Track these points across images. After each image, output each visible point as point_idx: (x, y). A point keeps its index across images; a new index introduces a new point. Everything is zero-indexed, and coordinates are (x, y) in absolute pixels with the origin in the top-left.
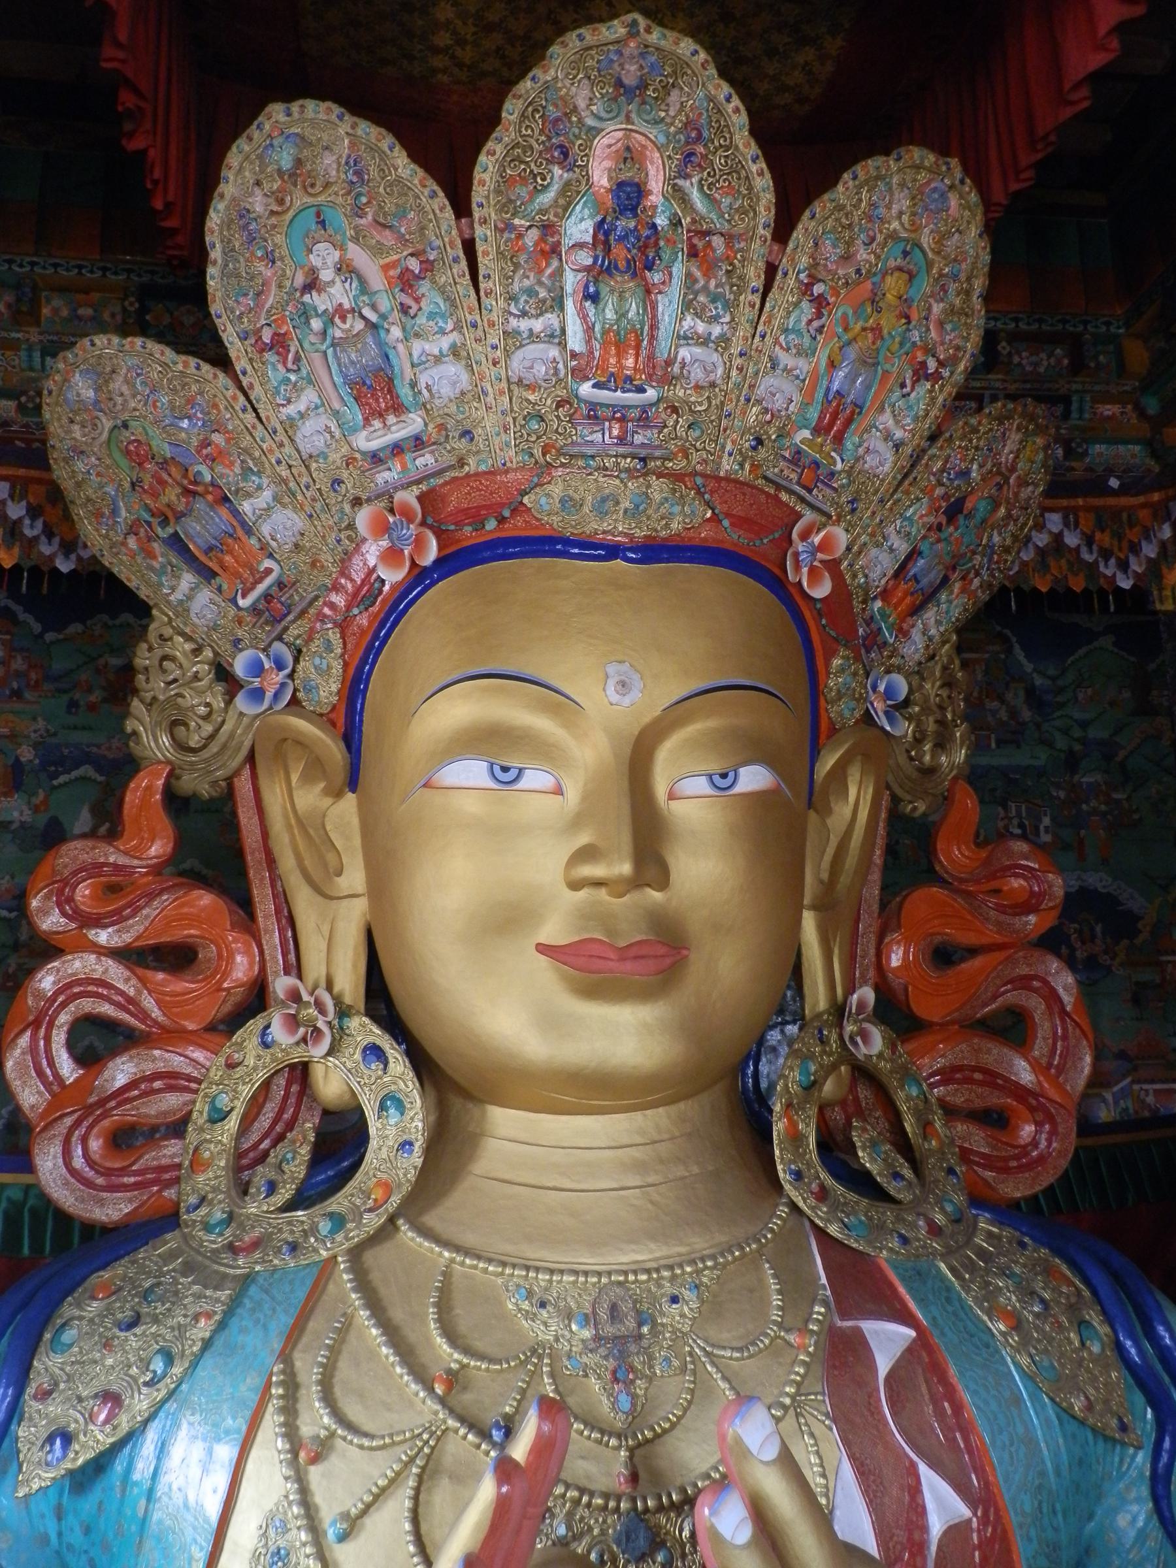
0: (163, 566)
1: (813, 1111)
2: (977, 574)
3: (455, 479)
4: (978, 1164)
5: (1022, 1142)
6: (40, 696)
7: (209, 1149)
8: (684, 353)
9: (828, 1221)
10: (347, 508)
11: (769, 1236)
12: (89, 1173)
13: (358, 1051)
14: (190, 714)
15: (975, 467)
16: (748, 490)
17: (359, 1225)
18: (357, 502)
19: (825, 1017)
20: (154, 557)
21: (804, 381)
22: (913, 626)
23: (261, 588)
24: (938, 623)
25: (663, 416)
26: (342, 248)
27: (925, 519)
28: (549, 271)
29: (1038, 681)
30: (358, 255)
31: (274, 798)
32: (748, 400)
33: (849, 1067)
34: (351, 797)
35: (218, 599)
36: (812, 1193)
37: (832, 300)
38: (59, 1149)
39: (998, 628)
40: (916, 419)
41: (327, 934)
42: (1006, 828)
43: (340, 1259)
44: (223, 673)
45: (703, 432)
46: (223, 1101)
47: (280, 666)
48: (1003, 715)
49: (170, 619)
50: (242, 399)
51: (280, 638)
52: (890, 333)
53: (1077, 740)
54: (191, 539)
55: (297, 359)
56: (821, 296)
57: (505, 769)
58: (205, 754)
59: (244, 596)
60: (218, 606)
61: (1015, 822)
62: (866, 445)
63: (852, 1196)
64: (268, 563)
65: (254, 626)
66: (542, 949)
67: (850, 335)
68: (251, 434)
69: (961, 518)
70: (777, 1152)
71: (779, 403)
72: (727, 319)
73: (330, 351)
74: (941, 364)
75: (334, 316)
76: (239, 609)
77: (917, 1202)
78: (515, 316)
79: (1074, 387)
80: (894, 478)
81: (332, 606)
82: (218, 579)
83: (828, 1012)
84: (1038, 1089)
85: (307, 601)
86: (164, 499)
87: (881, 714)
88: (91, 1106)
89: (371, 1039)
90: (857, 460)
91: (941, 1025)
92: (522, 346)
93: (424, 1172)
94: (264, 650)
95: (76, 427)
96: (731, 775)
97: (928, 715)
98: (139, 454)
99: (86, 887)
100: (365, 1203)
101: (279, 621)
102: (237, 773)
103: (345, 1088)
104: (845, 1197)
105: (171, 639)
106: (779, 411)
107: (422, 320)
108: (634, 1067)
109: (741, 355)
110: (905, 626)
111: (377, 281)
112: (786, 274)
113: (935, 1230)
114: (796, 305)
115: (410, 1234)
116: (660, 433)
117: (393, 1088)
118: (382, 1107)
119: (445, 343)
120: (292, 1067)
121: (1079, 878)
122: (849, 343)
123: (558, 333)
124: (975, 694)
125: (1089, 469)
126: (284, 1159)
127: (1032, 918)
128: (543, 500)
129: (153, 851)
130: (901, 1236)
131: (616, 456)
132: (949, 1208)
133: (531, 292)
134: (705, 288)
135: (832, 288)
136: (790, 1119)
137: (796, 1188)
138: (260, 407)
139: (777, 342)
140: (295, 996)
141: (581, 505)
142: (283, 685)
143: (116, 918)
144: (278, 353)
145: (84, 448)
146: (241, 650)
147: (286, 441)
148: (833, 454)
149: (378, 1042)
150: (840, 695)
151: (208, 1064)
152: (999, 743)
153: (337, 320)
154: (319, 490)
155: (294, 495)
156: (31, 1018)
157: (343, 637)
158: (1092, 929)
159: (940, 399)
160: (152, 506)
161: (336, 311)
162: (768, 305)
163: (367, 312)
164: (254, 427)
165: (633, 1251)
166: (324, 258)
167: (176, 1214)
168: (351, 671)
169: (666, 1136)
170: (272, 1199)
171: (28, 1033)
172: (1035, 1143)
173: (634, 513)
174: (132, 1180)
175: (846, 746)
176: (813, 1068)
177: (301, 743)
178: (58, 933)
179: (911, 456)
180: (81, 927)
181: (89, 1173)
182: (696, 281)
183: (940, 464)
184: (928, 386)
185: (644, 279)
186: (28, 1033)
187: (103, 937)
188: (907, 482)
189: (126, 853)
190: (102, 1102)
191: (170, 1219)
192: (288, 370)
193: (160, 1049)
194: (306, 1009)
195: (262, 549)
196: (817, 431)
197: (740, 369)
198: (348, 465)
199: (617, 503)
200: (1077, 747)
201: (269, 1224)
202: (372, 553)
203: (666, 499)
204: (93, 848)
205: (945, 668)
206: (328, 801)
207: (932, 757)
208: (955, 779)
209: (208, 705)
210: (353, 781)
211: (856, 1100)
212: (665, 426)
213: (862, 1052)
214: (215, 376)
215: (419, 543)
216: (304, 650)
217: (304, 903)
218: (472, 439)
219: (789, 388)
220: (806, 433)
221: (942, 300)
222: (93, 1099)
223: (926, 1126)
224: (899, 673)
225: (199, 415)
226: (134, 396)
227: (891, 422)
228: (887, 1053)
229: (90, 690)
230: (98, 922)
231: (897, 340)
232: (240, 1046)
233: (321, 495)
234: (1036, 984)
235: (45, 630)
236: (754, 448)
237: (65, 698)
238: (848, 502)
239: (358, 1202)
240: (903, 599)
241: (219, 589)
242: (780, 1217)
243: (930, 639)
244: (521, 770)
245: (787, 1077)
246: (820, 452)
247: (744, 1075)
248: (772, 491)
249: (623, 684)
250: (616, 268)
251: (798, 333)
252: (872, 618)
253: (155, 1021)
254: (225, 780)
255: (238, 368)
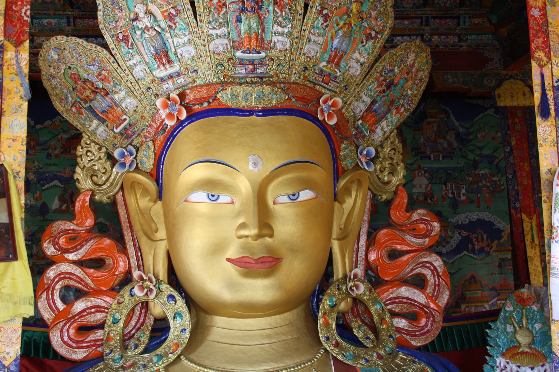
0: (86, 118)
1: (335, 315)
2: (402, 106)
3: (193, 87)
4: (404, 334)
5: (421, 325)
6: (35, 152)
7: (113, 333)
8: (275, 39)
9: (338, 354)
10: (153, 98)
11: (315, 360)
12: (70, 343)
13: (166, 297)
14: (98, 172)
15: (396, 68)
16: (301, 87)
17: (168, 359)
18: (157, 95)
19: (341, 280)
20: (83, 115)
21: (322, 45)
22: (376, 128)
23: (122, 126)
24: (388, 126)
25: (268, 62)
26: (147, 5)
27: (377, 89)
28: (222, 13)
29: (461, 130)
30: (153, 8)
31: (131, 201)
32: (300, 54)
33: (351, 299)
34: (160, 202)
35: (107, 130)
36: (333, 345)
37: (331, 15)
38: (59, 334)
39: (444, 107)
40: (369, 54)
41: (153, 254)
42: (446, 194)
43: (161, 370)
44: (110, 157)
45: (283, 67)
46: (117, 316)
47: (131, 154)
48: (445, 145)
49: (89, 137)
50: (112, 58)
51: (131, 144)
52: (355, 25)
53: (478, 155)
54: (96, 108)
55: (132, 45)
56: (327, 14)
57: (213, 196)
58: (105, 187)
59: (116, 128)
60: (107, 132)
61: (450, 192)
62: (349, 65)
63: (349, 346)
64: (124, 117)
65: (121, 139)
66: (228, 260)
67: (340, 26)
68: (116, 71)
69: (392, 86)
70: (319, 330)
71: (313, 53)
72: (290, 25)
73: (144, 42)
74: (377, 33)
75: (145, 29)
76: (115, 133)
77: (374, 347)
78: (211, 29)
79: (461, 12)
80: (362, 75)
81: (149, 133)
82: (106, 122)
83: (342, 278)
84: (427, 305)
85: (140, 130)
86: (85, 94)
87: (364, 163)
88: (70, 318)
89: (170, 293)
90: (346, 71)
91: (391, 282)
92: (214, 40)
93: (190, 339)
94: (125, 148)
95: (52, 68)
96: (297, 195)
97: (385, 162)
98: (76, 78)
99: (63, 238)
100: (169, 351)
101: (131, 137)
102: (117, 193)
103: (161, 310)
104: (345, 346)
105: (90, 144)
106: (313, 57)
107: (177, 31)
108: (262, 301)
109: (297, 38)
110: (373, 128)
111: (160, 17)
112: (312, 8)
113: (380, 357)
114: (317, 18)
115: (186, 361)
116: (267, 68)
117: (179, 310)
118: (175, 317)
119: (186, 39)
120: (142, 303)
121: (477, 215)
122: (339, 29)
123: (227, 34)
124: (433, 136)
125: (469, 46)
126: (140, 336)
127: (427, 240)
128: (224, 96)
129: (87, 224)
130: (366, 359)
131: (251, 78)
132: (387, 349)
133: (216, 20)
134: (281, 15)
135: (330, 11)
136: (325, 318)
137: (327, 343)
138: (119, 61)
139: (310, 32)
140: (141, 278)
141: (238, 97)
142: (133, 161)
143: (75, 249)
144: (125, 43)
145: (55, 76)
146: (116, 148)
147: (129, 73)
148: (336, 70)
149: (173, 294)
150: (345, 158)
151: (111, 302)
152: (443, 158)
153: (146, 31)
154: (143, 91)
155: (133, 93)
156: (46, 287)
157: (154, 144)
158: (482, 237)
159: (379, 45)
160: (81, 97)
161: (145, 28)
162: (305, 19)
163: (157, 28)
164: (118, 68)
165: (265, 365)
166: (140, 9)
167: (103, 356)
168: (157, 157)
169: (279, 325)
170: (136, 350)
171: (46, 292)
172: (426, 325)
173: (259, 99)
174: (86, 345)
175: (348, 177)
176: (335, 299)
177: (139, 183)
178: (54, 256)
179: (368, 67)
180: (62, 253)
181: (70, 343)
182: (277, 13)
183: (381, 68)
184: (373, 41)
185: (258, 13)
186: (46, 292)
187: (71, 256)
188: (367, 77)
189: (77, 225)
190: (73, 317)
191: (100, 358)
192: (129, 48)
193: (93, 297)
194: (145, 282)
195: (122, 112)
196: (328, 62)
197: (296, 43)
198: (152, 82)
199: (252, 96)
200: (477, 158)
201: (136, 359)
202: (163, 113)
203: (270, 93)
204: (65, 224)
205: (392, 143)
206: (152, 204)
207: (388, 178)
208: (398, 186)
209: (105, 168)
210: (160, 196)
211: (358, 311)
212: (269, 66)
213: (356, 293)
214: (102, 50)
215: (180, 112)
216: (140, 149)
217: (144, 243)
218: (197, 73)
219: (317, 48)
220: (324, 63)
221: (375, 10)
222: (70, 316)
223: (382, 320)
224: (372, 146)
225: (97, 64)
226: (72, 58)
227: (358, 56)
228: (368, 293)
229: (55, 149)
230: (68, 251)
231: (358, 26)
232: (122, 296)
233: (143, 93)
234: (428, 265)
235: (36, 124)
236: (304, 71)
237: (46, 152)
238: (344, 86)
239: (167, 350)
240: (370, 119)
241: (107, 126)
242: (320, 353)
243: (385, 132)
244: (218, 196)
245: (324, 303)
246: (331, 70)
247: (313, 302)
248: (312, 85)
249: (255, 163)
250: (247, 10)
251: (318, 28)
252: (358, 127)
253: (91, 288)
254: (113, 196)
255: (110, 48)
